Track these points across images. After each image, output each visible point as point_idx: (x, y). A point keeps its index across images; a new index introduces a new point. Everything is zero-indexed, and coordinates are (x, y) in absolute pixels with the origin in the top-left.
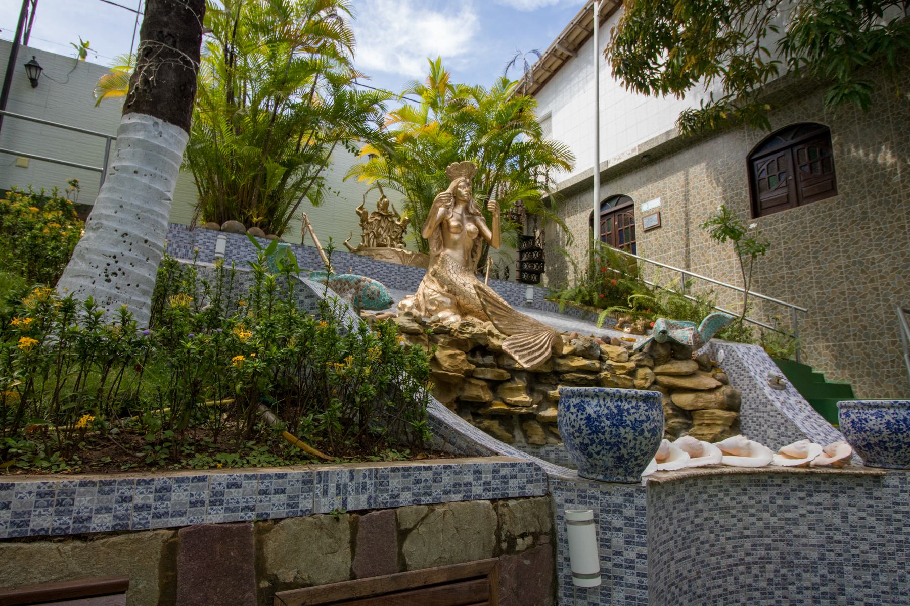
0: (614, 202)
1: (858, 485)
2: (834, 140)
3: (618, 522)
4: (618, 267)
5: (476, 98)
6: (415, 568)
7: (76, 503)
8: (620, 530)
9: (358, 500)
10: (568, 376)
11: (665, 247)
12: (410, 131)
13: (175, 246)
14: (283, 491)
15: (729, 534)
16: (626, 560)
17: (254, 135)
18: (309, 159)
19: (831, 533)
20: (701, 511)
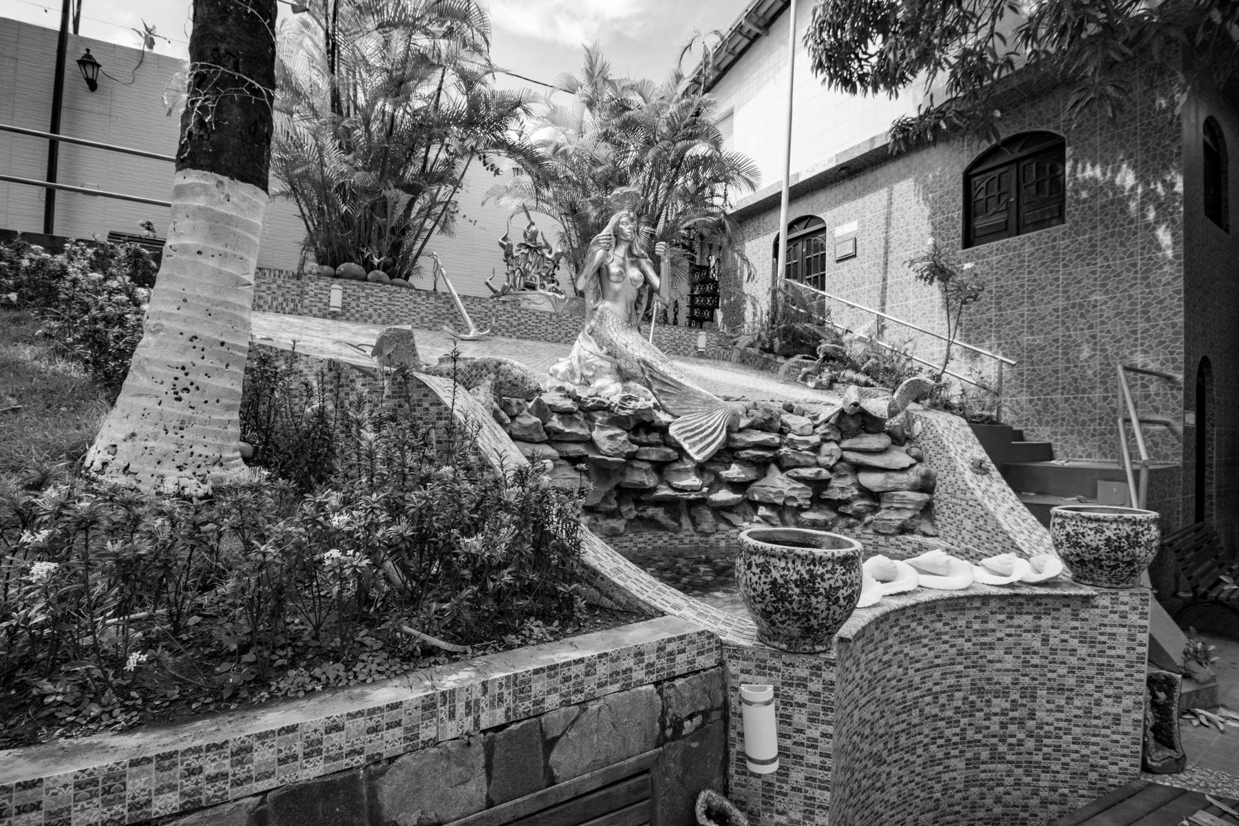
0: (803, 225)
1: (1065, 606)
2: (1069, 151)
3: (801, 697)
4: (805, 308)
5: (641, 95)
6: (565, 779)
7: (129, 787)
8: (803, 705)
9: (493, 715)
10: (743, 454)
11: (859, 281)
12: (561, 139)
13: (281, 299)
14: (398, 724)
15: (918, 665)
16: (808, 739)
17: (370, 151)
18: (441, 179)
19: (1028, 657)
20: (891, 646)
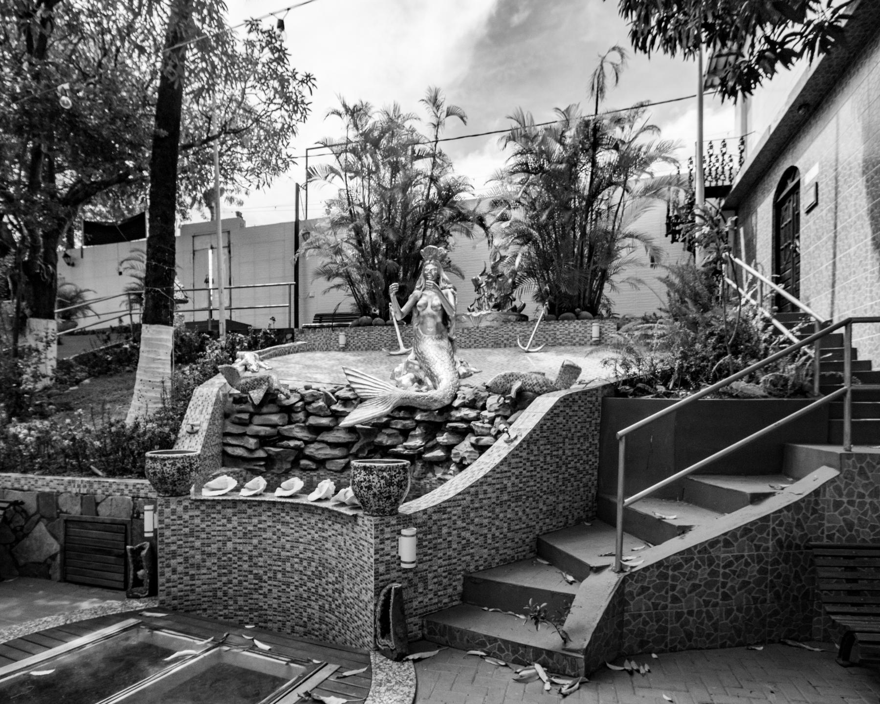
15: (288, 538)
